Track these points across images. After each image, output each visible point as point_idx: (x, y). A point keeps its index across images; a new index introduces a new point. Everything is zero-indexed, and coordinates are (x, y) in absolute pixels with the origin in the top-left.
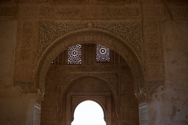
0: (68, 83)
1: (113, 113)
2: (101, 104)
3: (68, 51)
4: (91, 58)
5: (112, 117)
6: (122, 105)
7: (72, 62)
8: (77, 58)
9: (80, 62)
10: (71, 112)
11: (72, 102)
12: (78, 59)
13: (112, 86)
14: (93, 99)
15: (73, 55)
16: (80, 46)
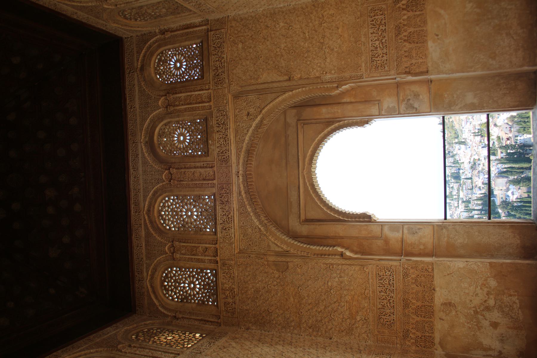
0: (265, 233)
1: (344, 100)
2: (322, 135)
5: (356, 102)
6: (317, 75)
10: (345, 221)
13: (268, 107)
14: (307, 160)
15: (195, 217)
16: (173, 200)
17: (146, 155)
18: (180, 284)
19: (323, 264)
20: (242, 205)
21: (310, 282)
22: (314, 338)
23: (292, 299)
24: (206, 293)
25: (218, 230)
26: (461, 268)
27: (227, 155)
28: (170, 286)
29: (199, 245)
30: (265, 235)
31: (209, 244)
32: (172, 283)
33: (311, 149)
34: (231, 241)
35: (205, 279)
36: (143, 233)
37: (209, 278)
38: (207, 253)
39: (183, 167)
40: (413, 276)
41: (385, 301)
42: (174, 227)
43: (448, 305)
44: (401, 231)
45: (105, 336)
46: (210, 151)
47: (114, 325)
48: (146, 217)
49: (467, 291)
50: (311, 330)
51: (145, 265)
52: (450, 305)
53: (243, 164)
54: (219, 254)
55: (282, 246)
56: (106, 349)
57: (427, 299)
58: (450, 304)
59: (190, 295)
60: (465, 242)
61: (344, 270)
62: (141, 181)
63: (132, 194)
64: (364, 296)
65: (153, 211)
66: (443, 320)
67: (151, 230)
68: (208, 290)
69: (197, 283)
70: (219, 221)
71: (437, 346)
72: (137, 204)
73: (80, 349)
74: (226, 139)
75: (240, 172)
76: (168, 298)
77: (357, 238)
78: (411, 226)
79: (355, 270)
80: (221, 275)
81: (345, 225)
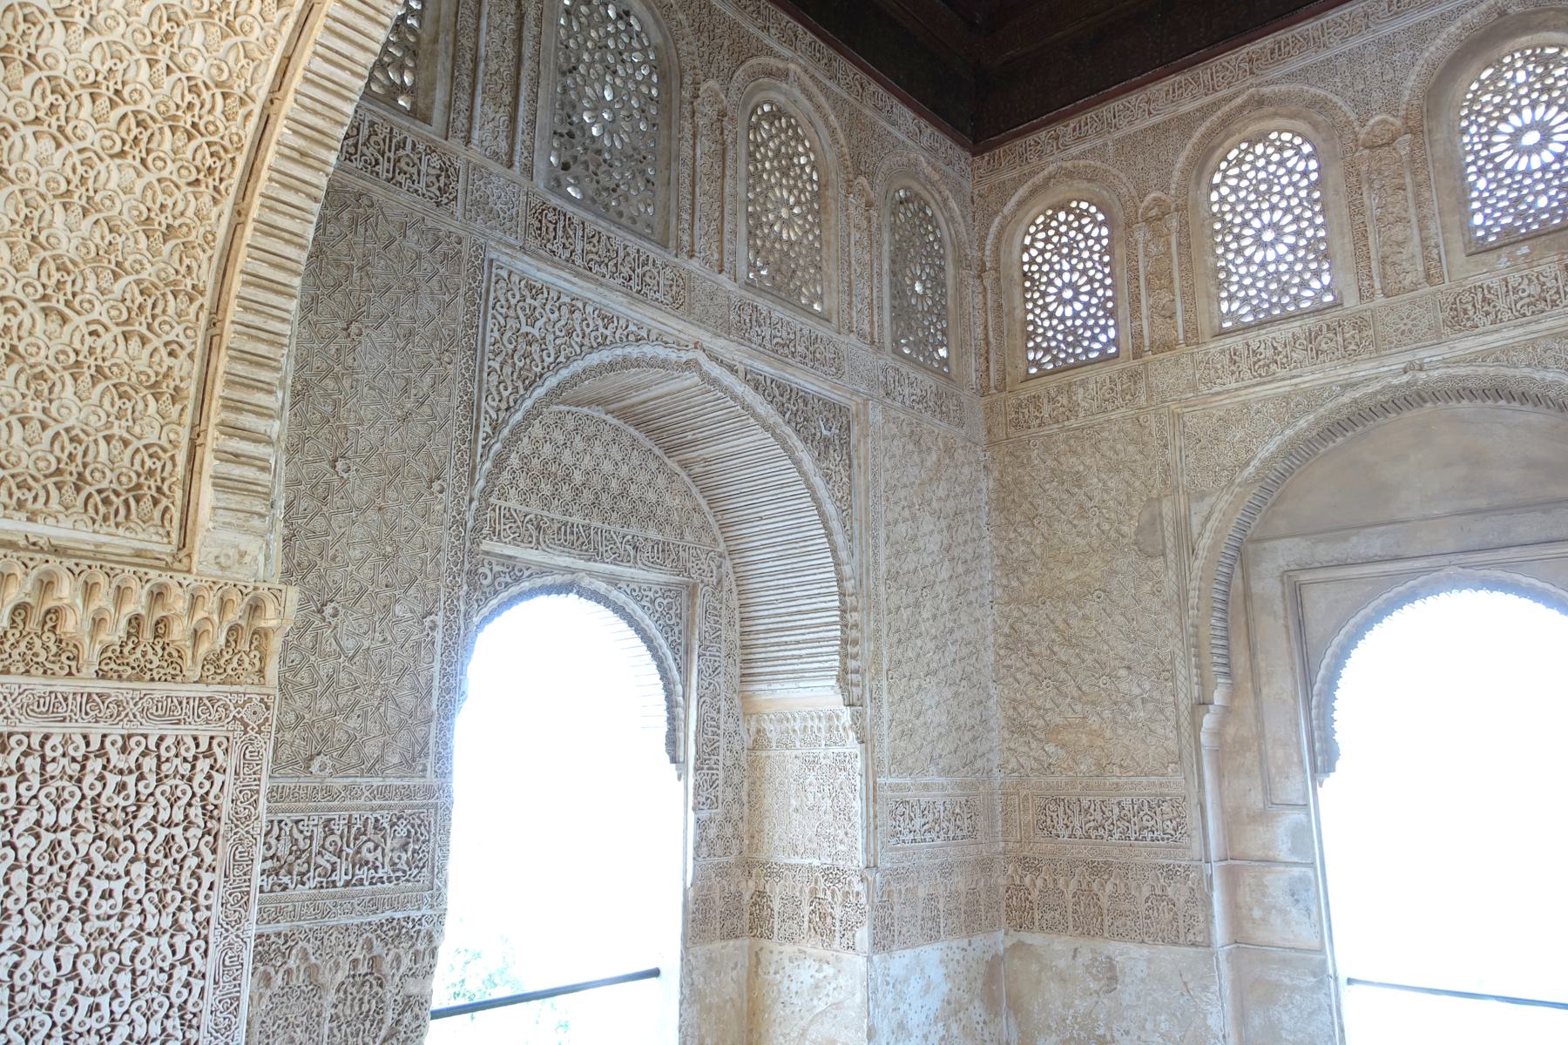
3: (1217, 232)
4: (1416, 231)
7: (1255, 311)
8: (1291, 265)
9: (1327, 289)
10: (1308, 700)
11: (1301, 624)
12: (1306, 269)
14: (1499, 574)
15: (1258, 258)
16: (1305, 174)
17: (1452, 29)
18: (1069, 256)
19: (1172, 653)
20: (1312, 398)
21: (1120, 619)
22: (991, 639)
23: (1072, 576)
24: (1054, 338)
25: (1229, 342)
26: (1205, 1018)
27: (1478, 318)
28: (1058, 233)
29: (1177, 292)
30: (1231, 482)
31: (1185, 321)
32: (1066, 234)
33: (1539, 584)
34: (1202, 387)
35: (1091, 328)
36: (1188, 107)
37: (1094, 338)
38: (1159, 320)
39: (1421, 178)
40: (1170, 891)
41: (1099, 817)
42: (1223, 200)
43: (1111, 976)
44: (1295, 859)
45: (884, 123)
46: (1491, 257)
47: (923, 123)
48: (1239, 101)
49: (1149, 1026)
50: (1006, 630)
51: (1099, 142)
52: (1110, 979)
53: (1451, 377)
54: (1161, 356)
55: (1207, 534)
56: (845, 150)
57: (1119, 923)
58: (1113, 979)
59: (1044, 294)
60: (1284, 1034)
61: (1162, 711)
62: (1354, 43)
63: (1308, 27)
64: (1104, 762)
65: (1261, 118)
66: (1074, 957)
67: (1202, 130)
68: (1065, 341)
69: (1078, 306)
70: (1253, 338)
71: (1015, 937)
72: (1277, 55)
73: (828, 83)
74: (1541, 305)
75: (1423, 375)
76: (1028, 233)
77: (1261, 736)
78: (1313, 889)
79: (1167, 739)
80: (1105, 372)
81: (1295, 699)
